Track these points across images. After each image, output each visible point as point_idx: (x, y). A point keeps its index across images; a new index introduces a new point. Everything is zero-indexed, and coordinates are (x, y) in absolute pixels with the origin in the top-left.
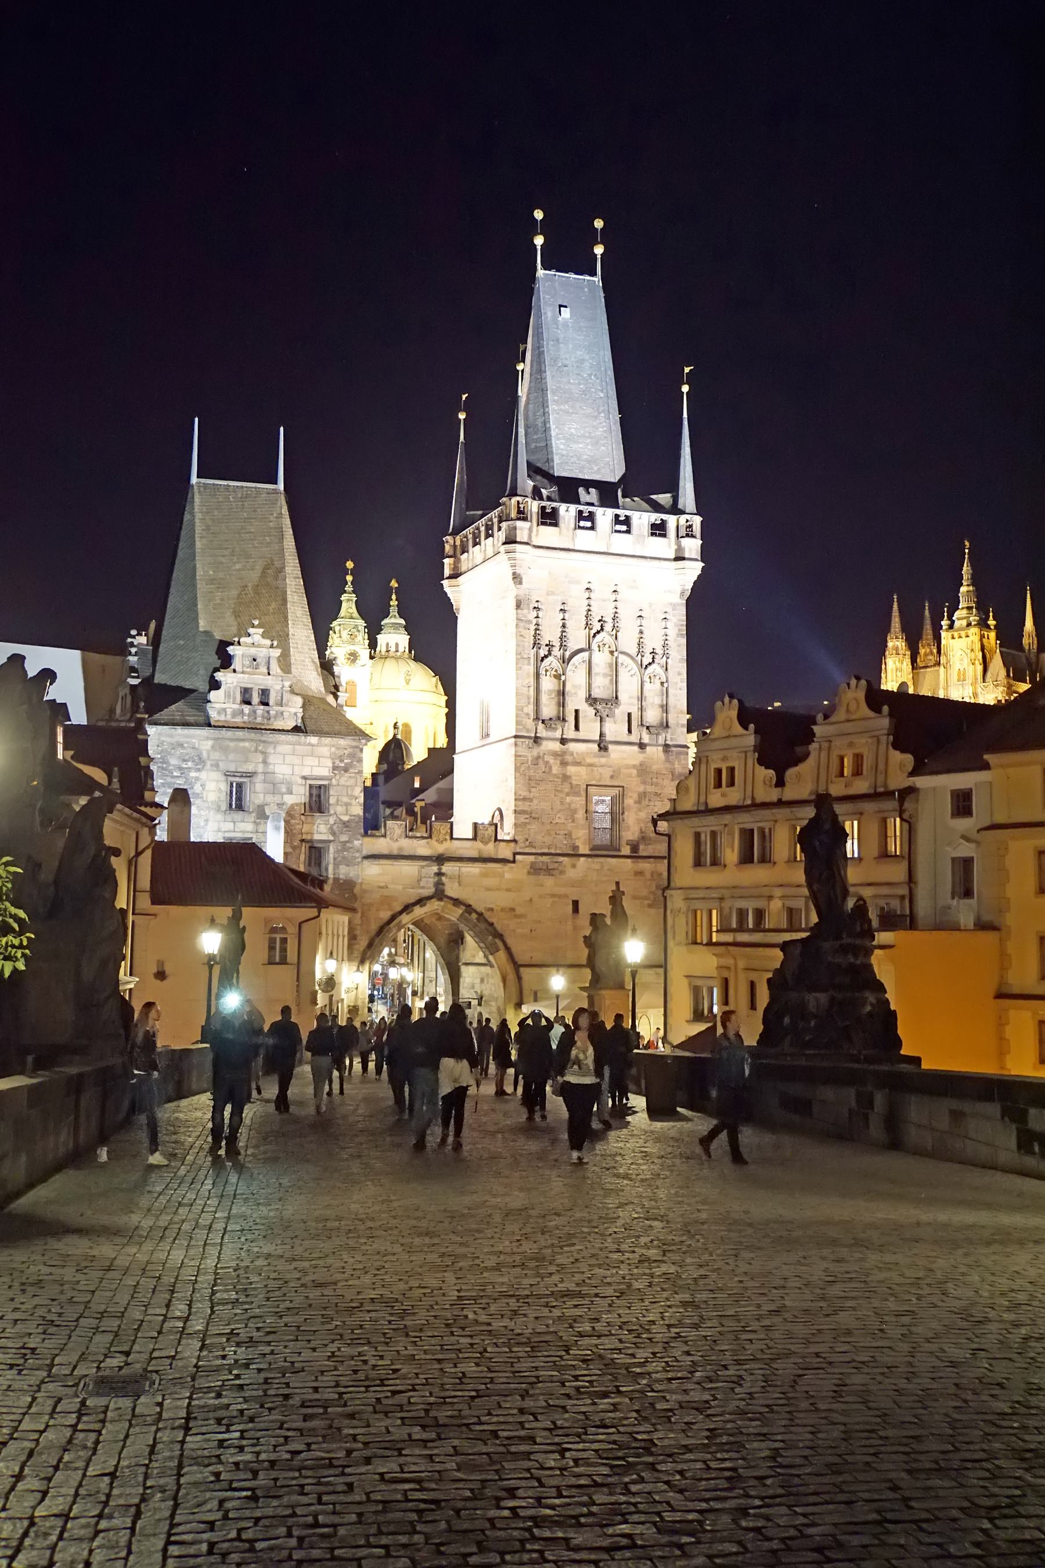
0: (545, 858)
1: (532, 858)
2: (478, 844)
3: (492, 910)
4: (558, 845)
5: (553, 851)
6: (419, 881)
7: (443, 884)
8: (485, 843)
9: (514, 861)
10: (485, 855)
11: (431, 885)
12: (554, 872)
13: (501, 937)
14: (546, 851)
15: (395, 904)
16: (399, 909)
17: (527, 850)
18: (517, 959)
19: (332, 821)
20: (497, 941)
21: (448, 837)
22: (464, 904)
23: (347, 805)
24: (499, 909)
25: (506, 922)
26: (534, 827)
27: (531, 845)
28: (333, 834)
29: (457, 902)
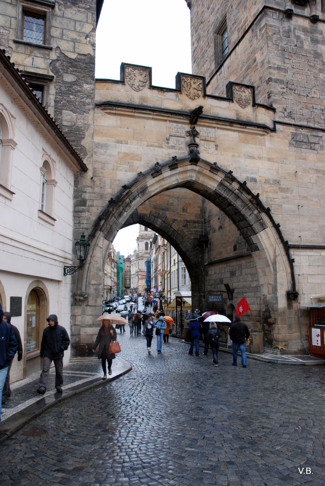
0: (304, 131)
1: (292, 130)
2: (234, 106)
3: (255, 180)
4: (317, 119)
5: (312, 125)
6: (168, 140)
7: (197, 145)
8: (244, 106)
9: (274, 130)
10: (244, 119)
11: (183, 145)
12: (317, 146)
13: (268, 212)
14: (304, 123)
15: (136, 163)
16: (143, 169)
17: (287, 120)
18: (286, 237)
19: (54, 56)
20: (264, 216)
21: (200, 93)
22: (223, 171)
23: (74, 41)
24: (263, 181)
25: (271, 195)
26: (291, 97)
27: (290, 115)
28: (56, 71)
29: (214, 168)
